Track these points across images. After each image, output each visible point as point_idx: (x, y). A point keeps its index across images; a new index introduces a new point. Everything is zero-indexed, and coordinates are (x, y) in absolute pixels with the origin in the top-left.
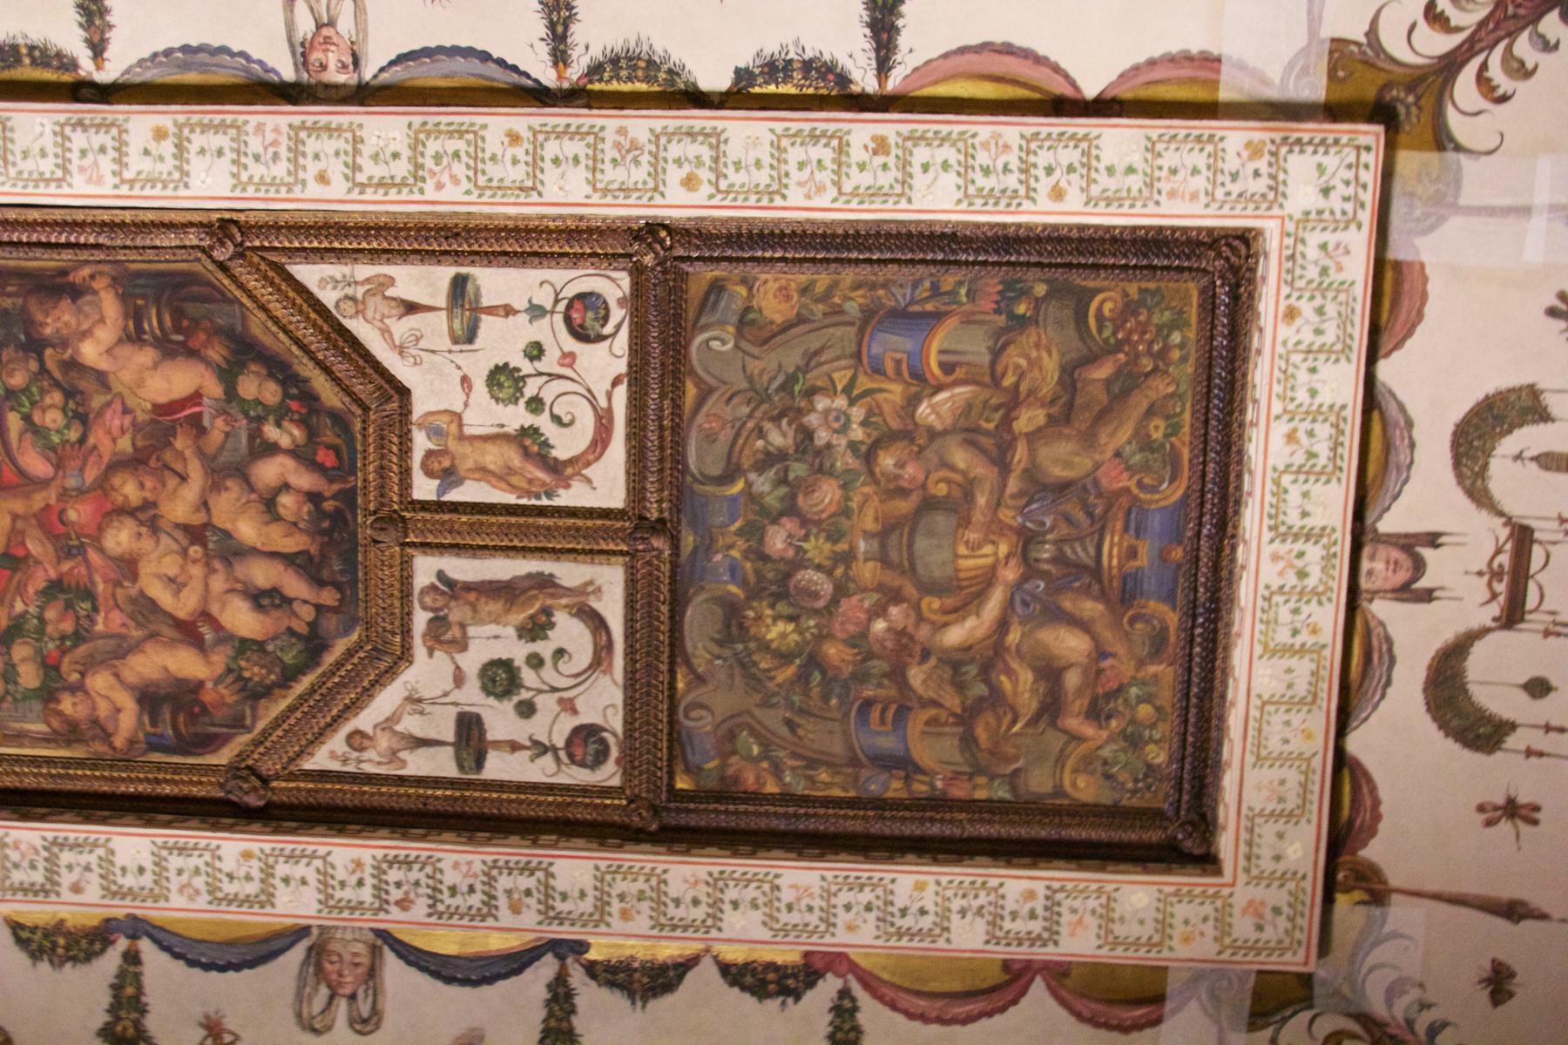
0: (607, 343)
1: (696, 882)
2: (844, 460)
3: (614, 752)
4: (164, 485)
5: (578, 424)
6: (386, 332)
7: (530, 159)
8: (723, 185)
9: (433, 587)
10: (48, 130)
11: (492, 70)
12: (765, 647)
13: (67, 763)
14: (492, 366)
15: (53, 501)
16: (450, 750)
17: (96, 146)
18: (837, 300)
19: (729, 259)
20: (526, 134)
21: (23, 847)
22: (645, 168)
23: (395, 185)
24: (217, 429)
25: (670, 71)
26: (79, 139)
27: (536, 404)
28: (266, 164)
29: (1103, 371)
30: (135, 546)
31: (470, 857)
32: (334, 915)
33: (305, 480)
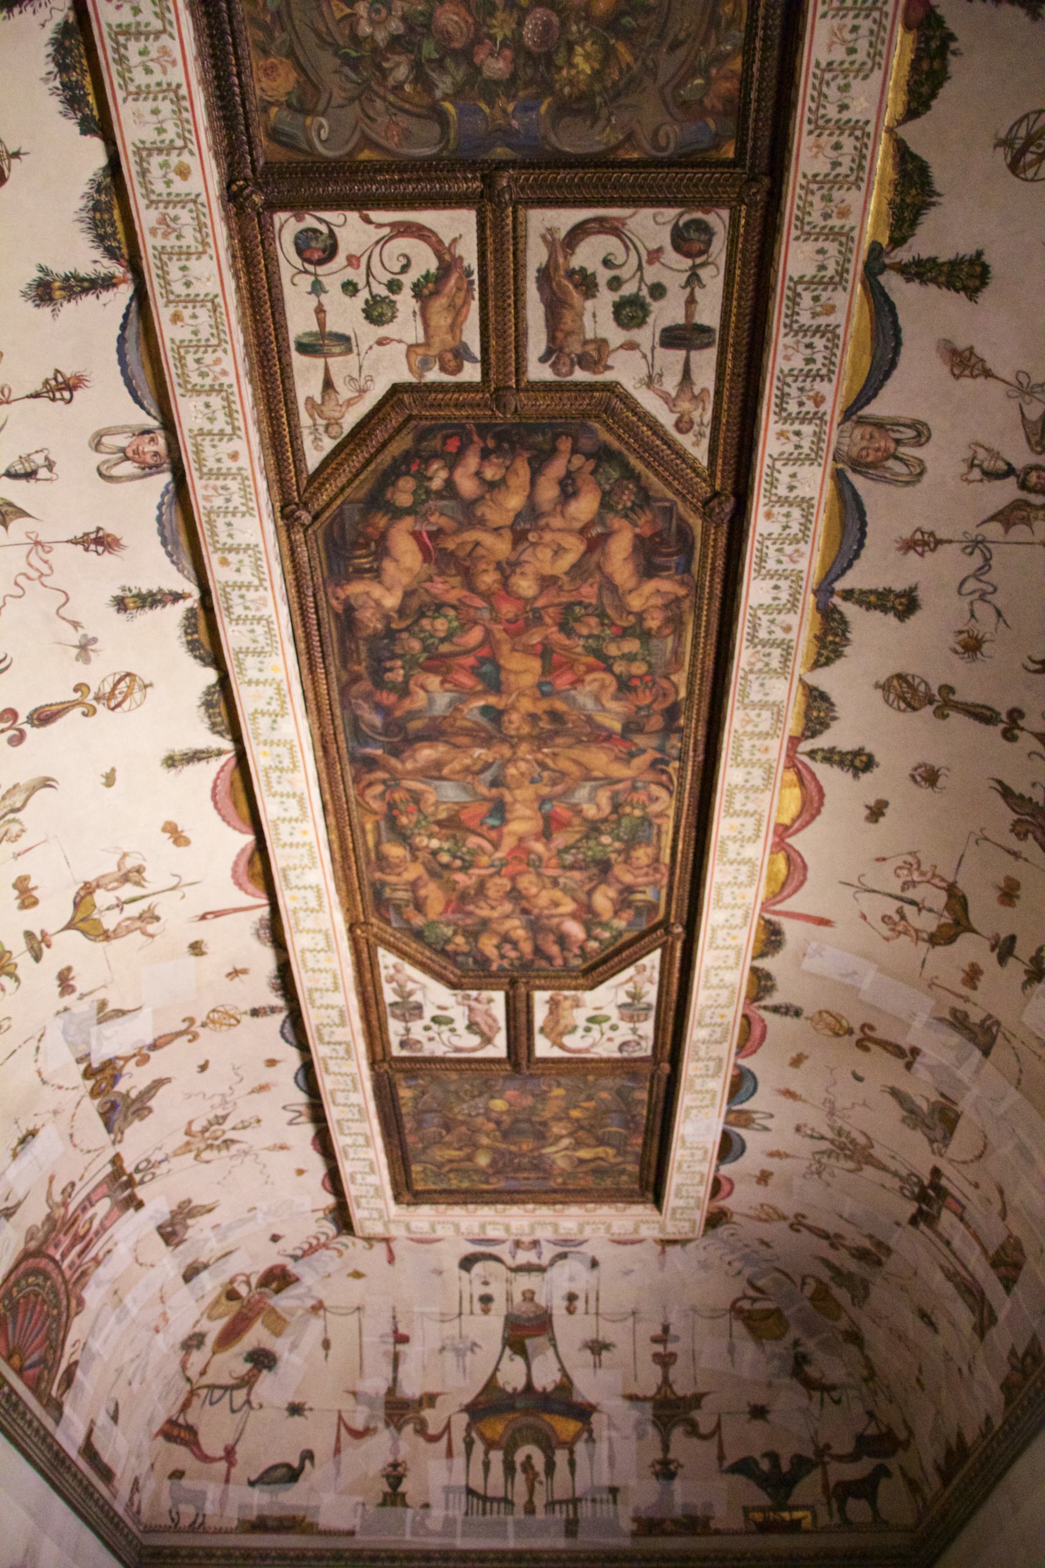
0: (336, 230)
1: (818, 146)
3: (698, 215)
4: (483, 557)
5: (407, 251)
6: (350, 403)
7: (190, 305)
8: (179, 143)
9: (553, 366)
10: (236, 628)
11: (132, 332)
12: (598, 75)
13: (697, 626)
14: (366, 323)
15: (501, 627)
16: (694, 354)
17: (240, 601)
18: (268, 19)
19: (247, 127)
20: (172, 309)
21: (753, 660)
22: (178, 211)
23: (229, 406)
24: (437, 521)
25: (98, 191)
26: (238, 611)
27: (394, 286)
28: (231, 494)
30: (531, 577)
31: (780, 347)
32: (824, 455)
33: (472, 461)
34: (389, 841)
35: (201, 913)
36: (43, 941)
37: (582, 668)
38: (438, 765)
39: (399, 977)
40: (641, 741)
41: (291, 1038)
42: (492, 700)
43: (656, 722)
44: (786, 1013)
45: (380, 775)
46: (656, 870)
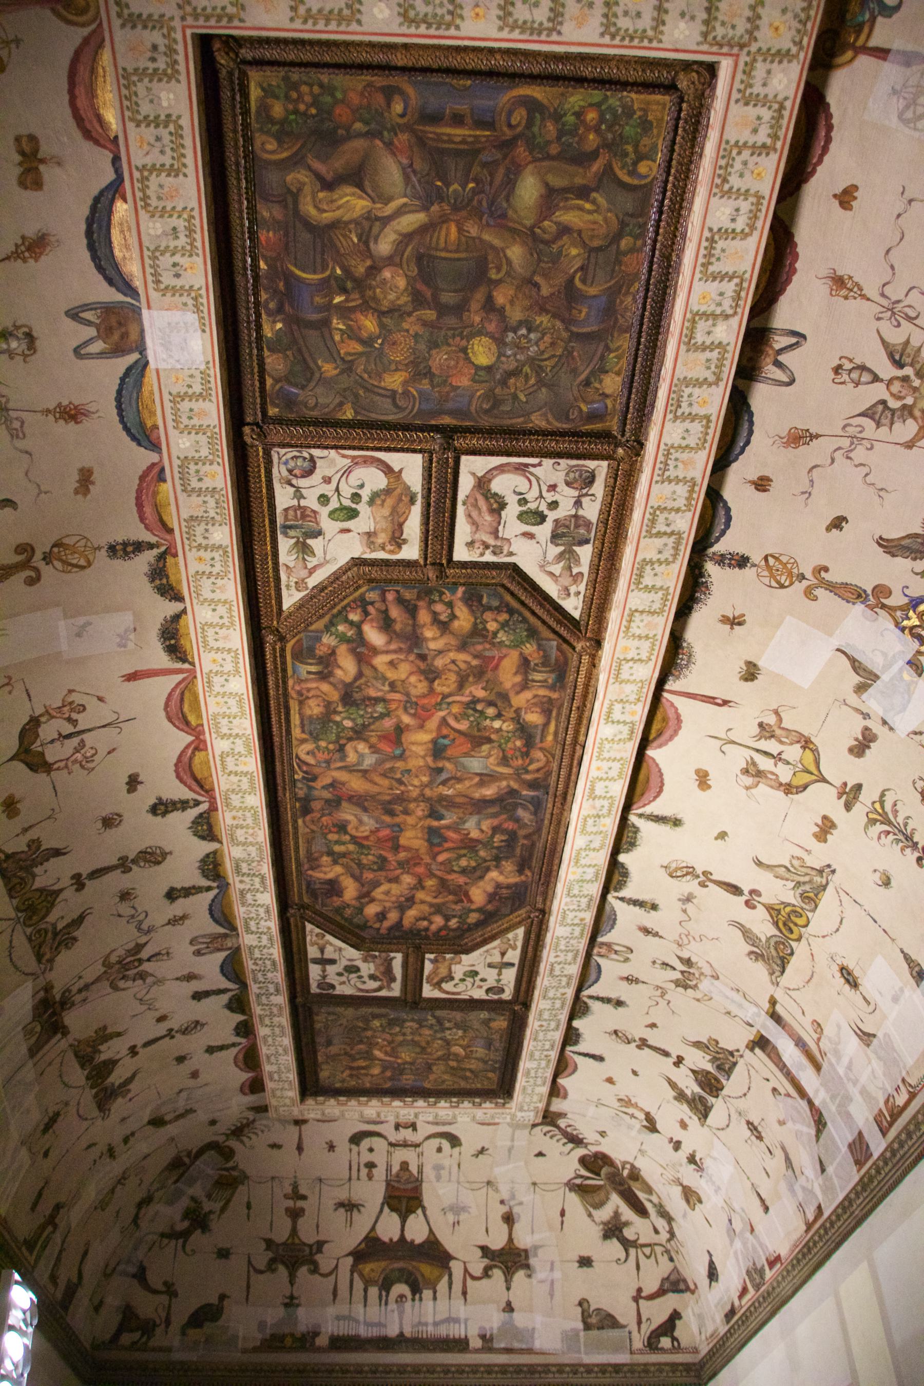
2: (439, 1035)
24: (458, 907)
29: (468, 1074)
34: (536, 726)
35: (725, 709)
36: (845, 793)
37: (372, 838)
38: (481, 784)
39: (566, 581)
40: (326, 795)
41: (722, 512)
42: (435, 823)
43: (316, 805)
44: (125, 544)
45: (528, 777)
46: (300, 693)
